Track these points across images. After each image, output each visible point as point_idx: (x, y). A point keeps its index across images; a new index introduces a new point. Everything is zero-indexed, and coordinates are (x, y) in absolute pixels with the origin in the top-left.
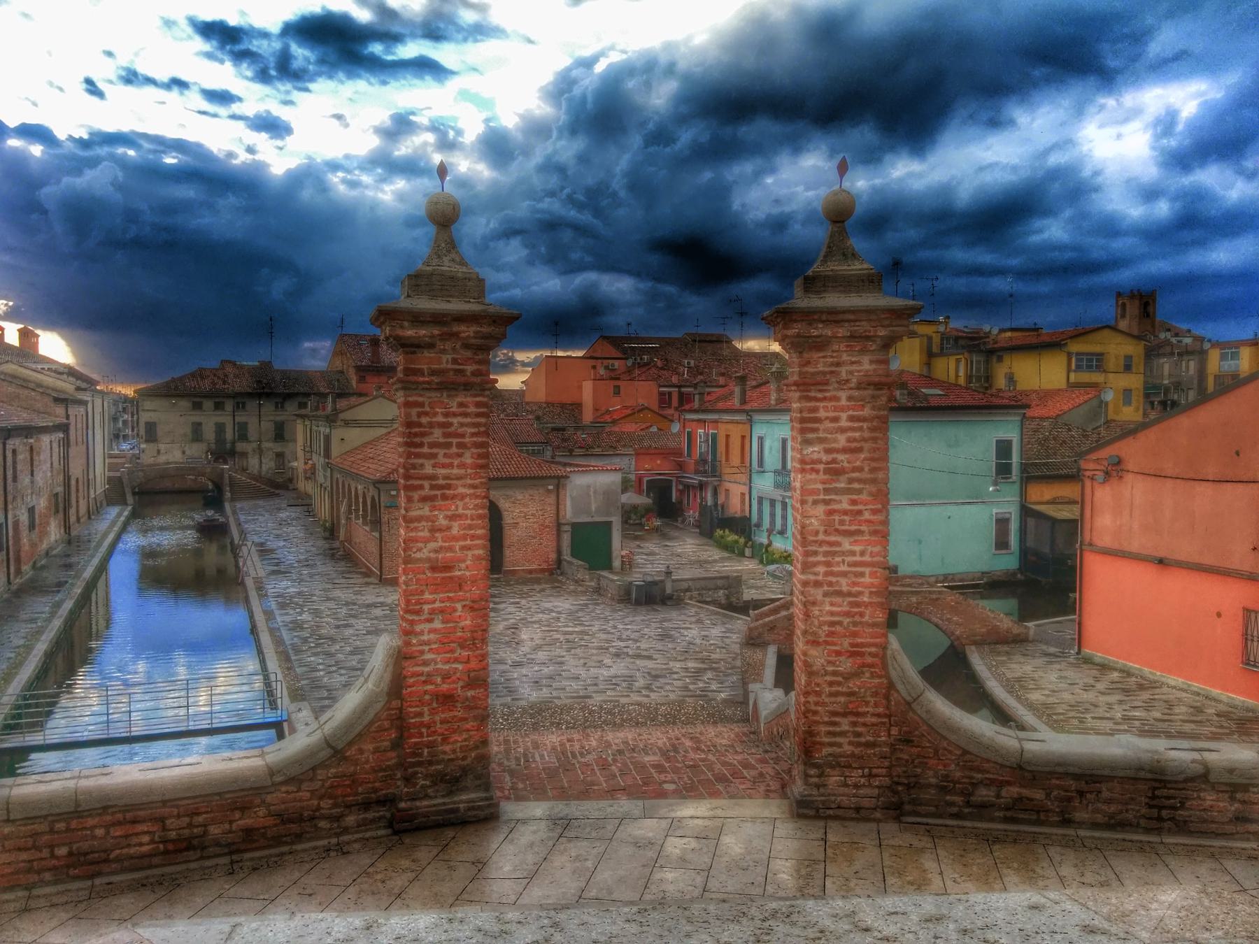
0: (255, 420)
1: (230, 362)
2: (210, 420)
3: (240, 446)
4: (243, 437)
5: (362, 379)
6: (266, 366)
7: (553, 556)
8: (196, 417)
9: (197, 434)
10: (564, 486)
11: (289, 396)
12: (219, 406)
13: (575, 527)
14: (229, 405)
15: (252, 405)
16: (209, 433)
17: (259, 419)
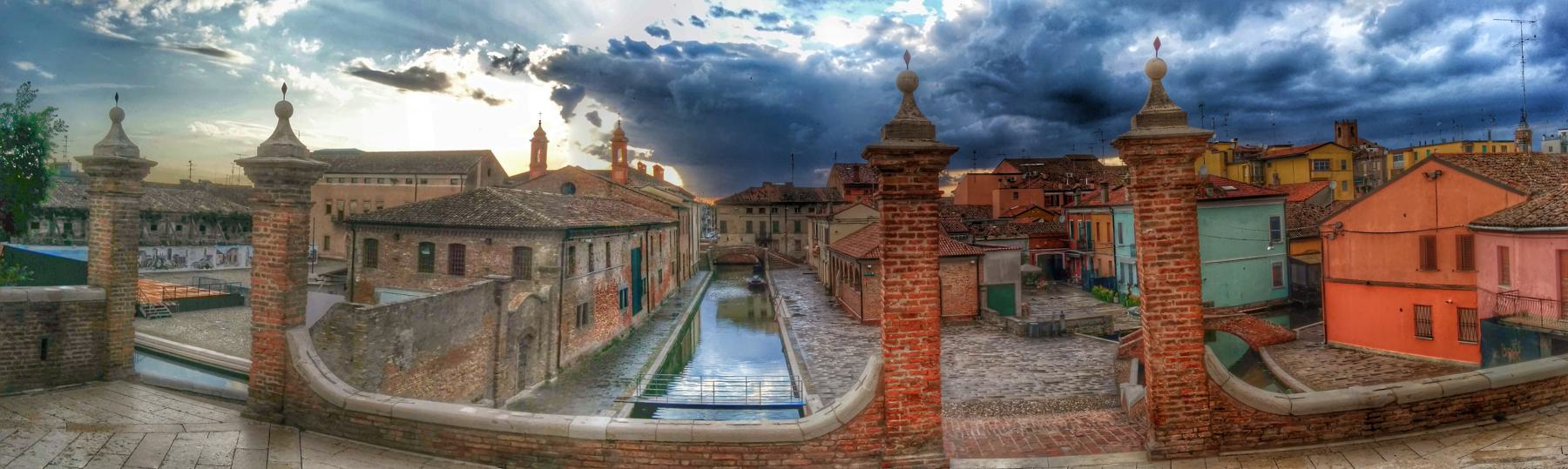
0: (784, 219)
1: (767, 183)
2: (756, 219)
3: (775, 236)
4: (776, 231)
5: (848, 193)
6: (789, 185)
7: (975, 307)
8: (749, 218)
9: (749, 229)
10: (982, 260)
11: (804, 204)
12: (762, 211)
13: (989, 287)
14: (768, 210)
15: (781, 209)
16: (756, 228)
17: (785, 219)
